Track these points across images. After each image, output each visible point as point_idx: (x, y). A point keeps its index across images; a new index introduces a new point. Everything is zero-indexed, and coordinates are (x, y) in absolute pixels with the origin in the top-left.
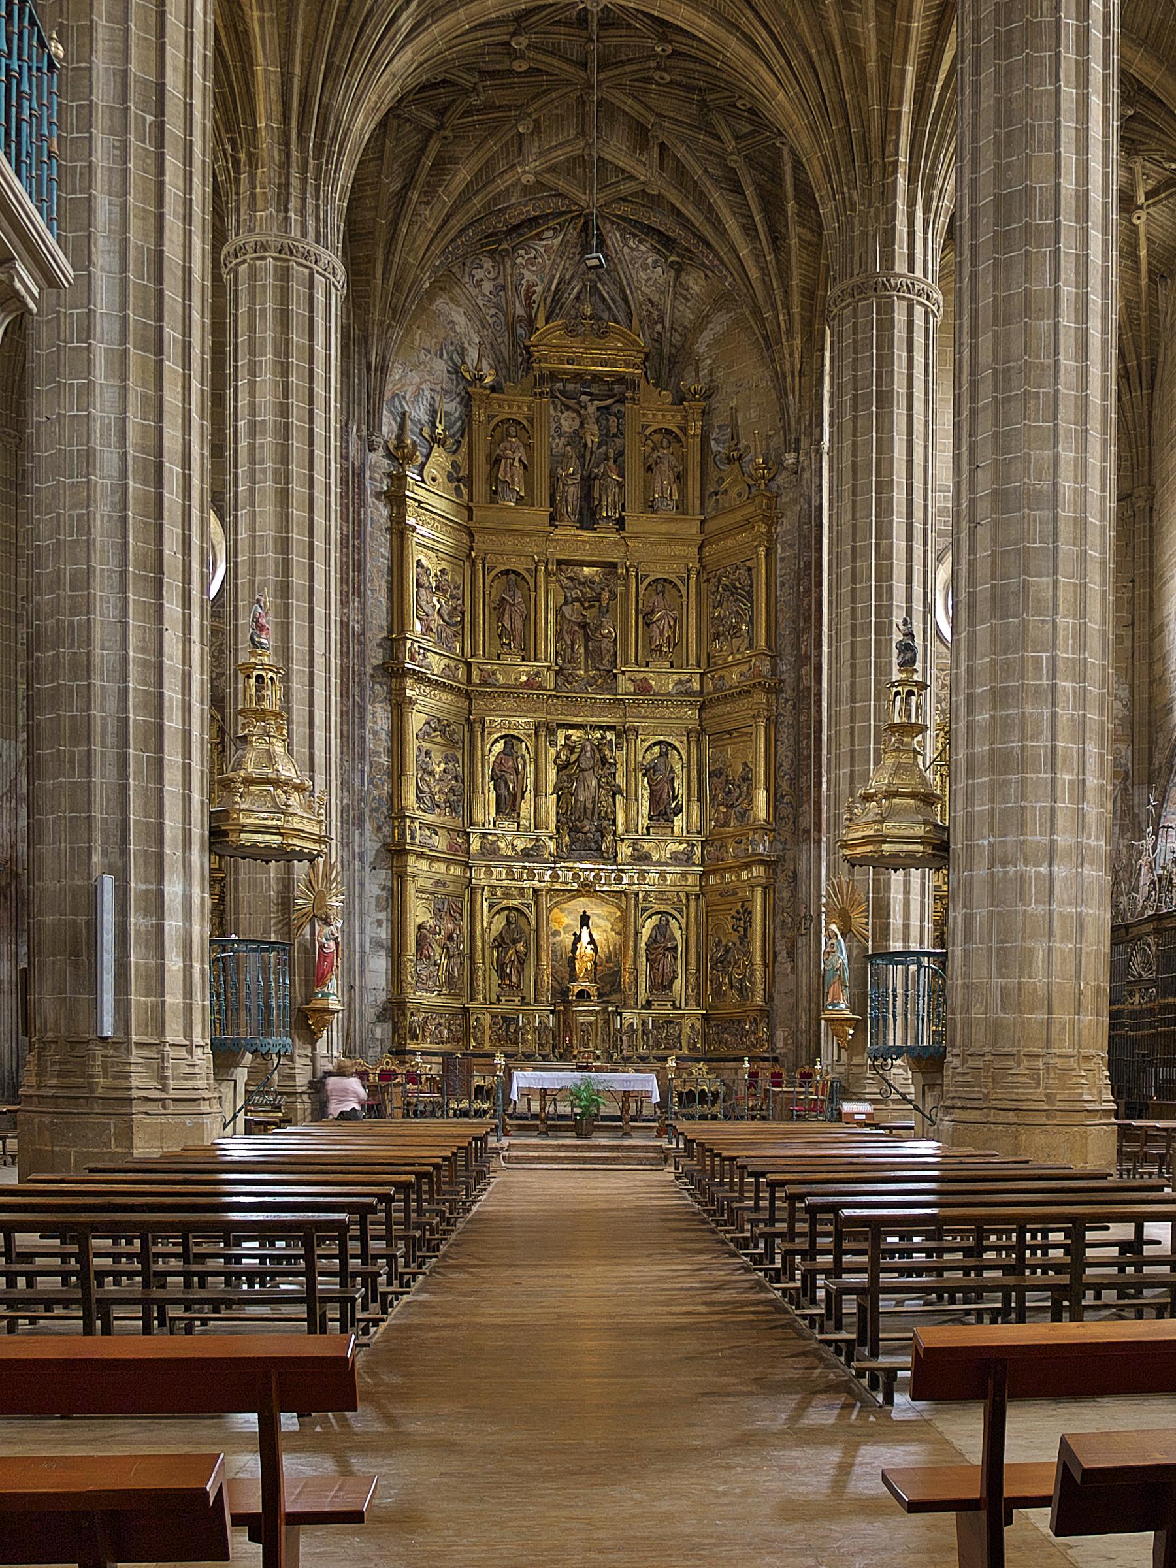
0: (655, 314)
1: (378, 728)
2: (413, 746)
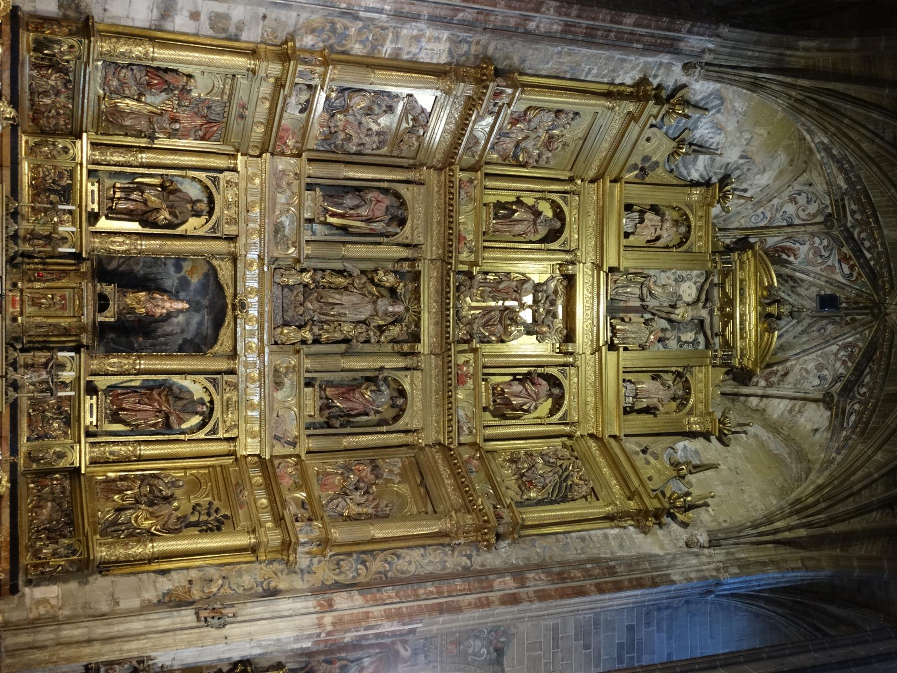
0: (774, 379)
1: (423, 44)
2: (399, 87)
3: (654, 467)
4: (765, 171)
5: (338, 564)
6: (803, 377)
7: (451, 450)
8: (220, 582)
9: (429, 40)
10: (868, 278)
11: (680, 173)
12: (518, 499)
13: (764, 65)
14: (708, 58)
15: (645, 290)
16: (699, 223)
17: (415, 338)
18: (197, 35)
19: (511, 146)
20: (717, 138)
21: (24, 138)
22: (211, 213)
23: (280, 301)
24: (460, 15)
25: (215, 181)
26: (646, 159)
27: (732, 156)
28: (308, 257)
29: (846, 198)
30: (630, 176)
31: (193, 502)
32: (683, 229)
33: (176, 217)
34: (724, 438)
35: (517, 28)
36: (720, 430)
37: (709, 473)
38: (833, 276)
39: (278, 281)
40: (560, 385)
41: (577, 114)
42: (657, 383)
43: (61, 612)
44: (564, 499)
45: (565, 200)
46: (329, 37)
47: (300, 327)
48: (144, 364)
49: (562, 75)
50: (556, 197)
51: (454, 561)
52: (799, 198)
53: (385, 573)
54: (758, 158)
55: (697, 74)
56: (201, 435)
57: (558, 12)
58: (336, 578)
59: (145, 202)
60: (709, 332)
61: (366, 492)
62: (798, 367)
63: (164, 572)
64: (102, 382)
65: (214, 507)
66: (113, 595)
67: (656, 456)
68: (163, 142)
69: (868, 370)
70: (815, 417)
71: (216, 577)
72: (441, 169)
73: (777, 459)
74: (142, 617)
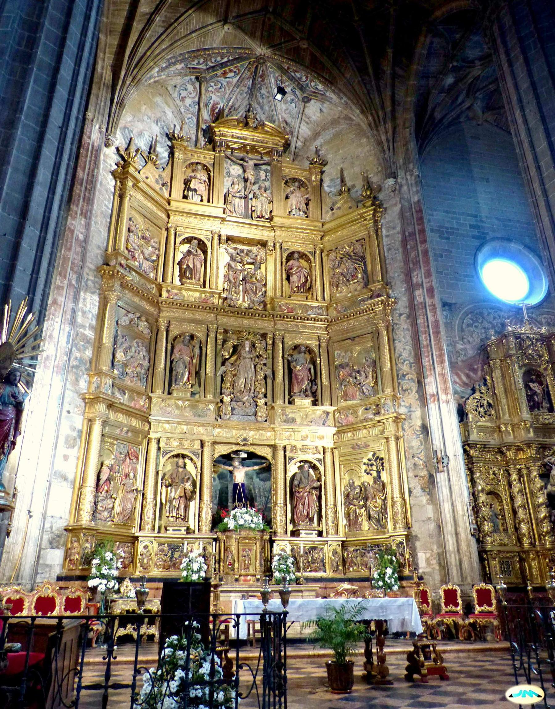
0: (288, 130)
1: (87, 309)
3: (343, 205)
4: (165, 112)
5: (405, 391)
6: (290, 113)
7: (331, 321)
8: (416, 459)
9: (85, 305)
10: (239, 62)
11: (164, 163)
12: (362, 284)
13: (109, 96)
14: (104, 130)
15: (238, 195)
16: (196, 157)
17: (264, 336)
18: (78, 458)
19: (148, 263)
20: (146, 136)
21: (138, 573)
22: (184, 456)
23: (241, 417)
24: (74, 282)
25: (165, 453)
26: (157, 182)
27: (156, 130)
28: (214, 397)
29: (189, 66)
30: (166, 195)
31: (364, 474)
32: (199, 167)
33: (189, 479)
34: (324, 163)
35: (83, 247)
36: (320, 164)
37: (346, 174)
38: (234, 83)
39: (228, 417)
40: (292, 253)
41: (130, 219)
42: (291, 196)
43: (435, 551)
44: (363, 258)
45: (180, 235)
46: (81, 370)
47: (257, 406)
48: (280, 501)
49: (108, 224)
50: (179, 240)
51: (404, 324)
52: (182, 95)
53: (410, 363)
54: (158, 115)
55: (113, 139)
56: (321, 468)
57: (74, 218)
58: (414, 392)
59: (180, 497)
60: (262, 162)
61: (359, 372)
62: (283, 114)
63: (410, 492)
64: (290, 527)
65: (367, 461)
66: (424, 521)
67: (335, 203)
68: (139, 485)
69: (292, 74)
70: (314, 109)
71: (413, 462)
72: (160, 310)
73: (336, 136)
74: (442, 504)
